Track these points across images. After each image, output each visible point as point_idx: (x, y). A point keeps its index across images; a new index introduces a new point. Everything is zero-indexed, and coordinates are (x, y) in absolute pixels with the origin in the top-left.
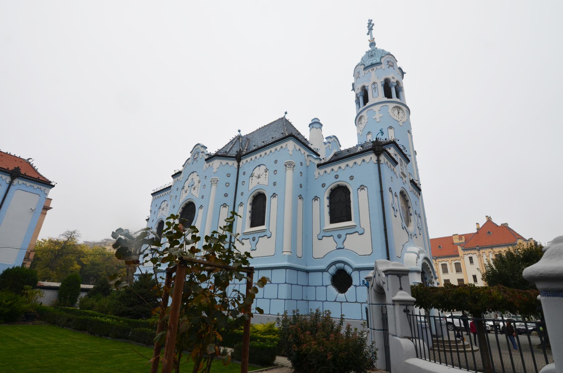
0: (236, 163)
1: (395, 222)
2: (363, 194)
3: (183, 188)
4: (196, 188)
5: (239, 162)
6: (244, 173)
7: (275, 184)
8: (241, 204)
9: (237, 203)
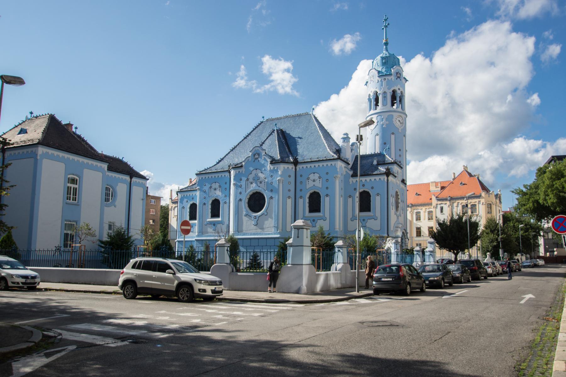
0: (294, 167)
1: (392, 211)
2: (378, 198)
3: (248, 179)
4: (263, 183)
5: (296, 165)
6: (301, 176)
7: (327, 188)
8: (301, 197)
9: (298, 196)
